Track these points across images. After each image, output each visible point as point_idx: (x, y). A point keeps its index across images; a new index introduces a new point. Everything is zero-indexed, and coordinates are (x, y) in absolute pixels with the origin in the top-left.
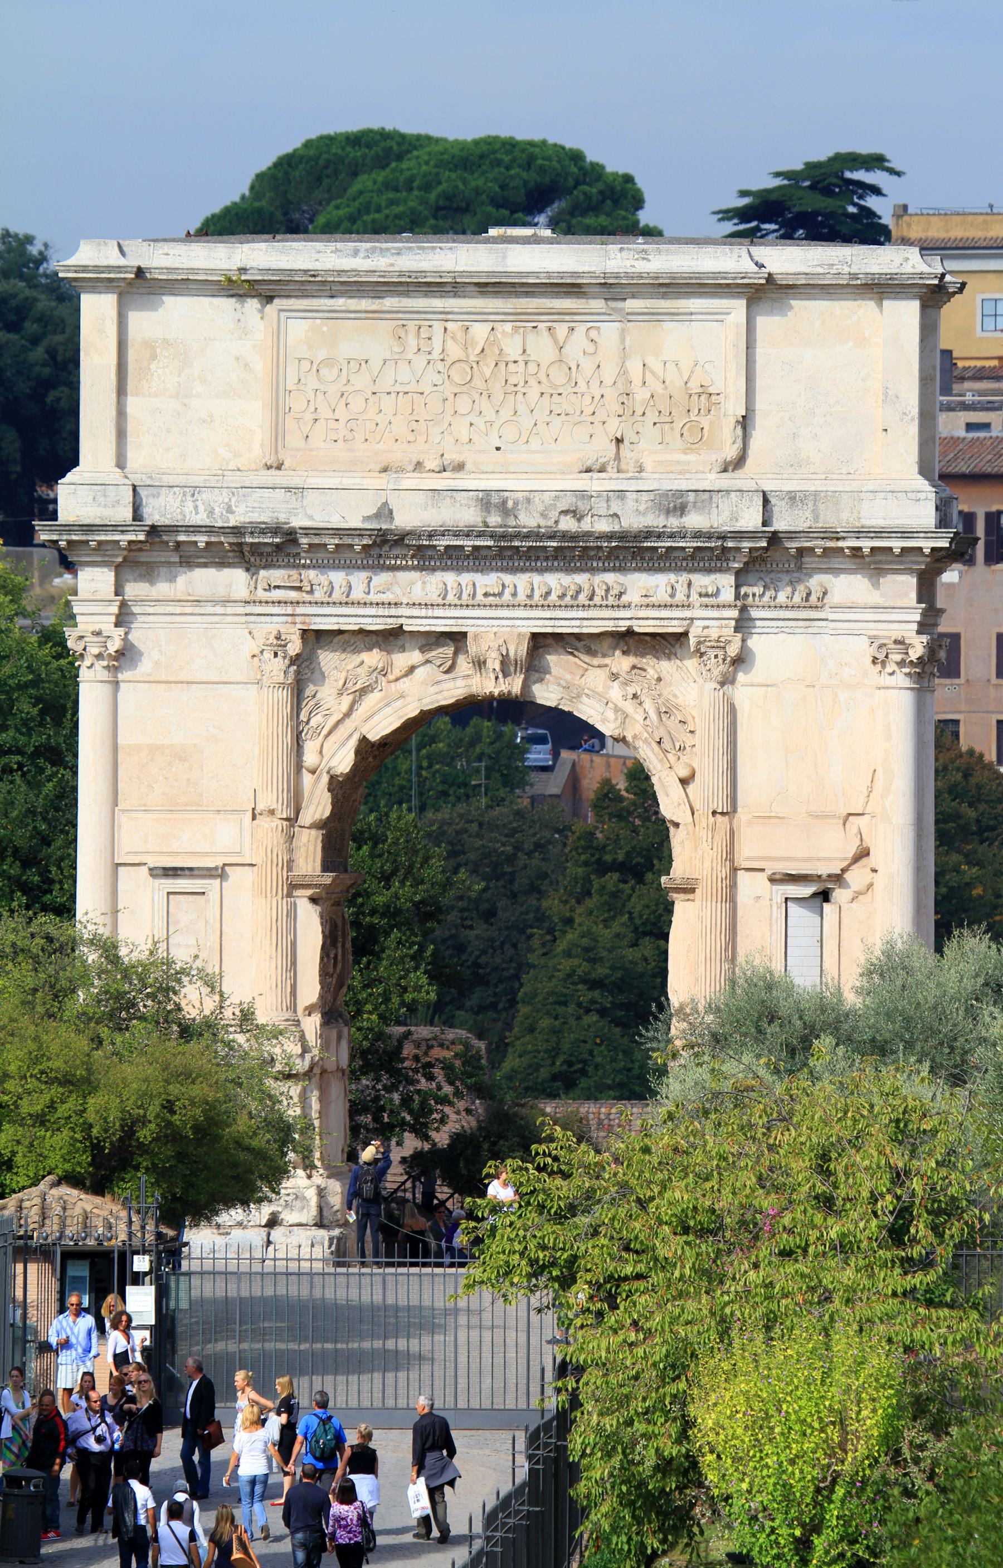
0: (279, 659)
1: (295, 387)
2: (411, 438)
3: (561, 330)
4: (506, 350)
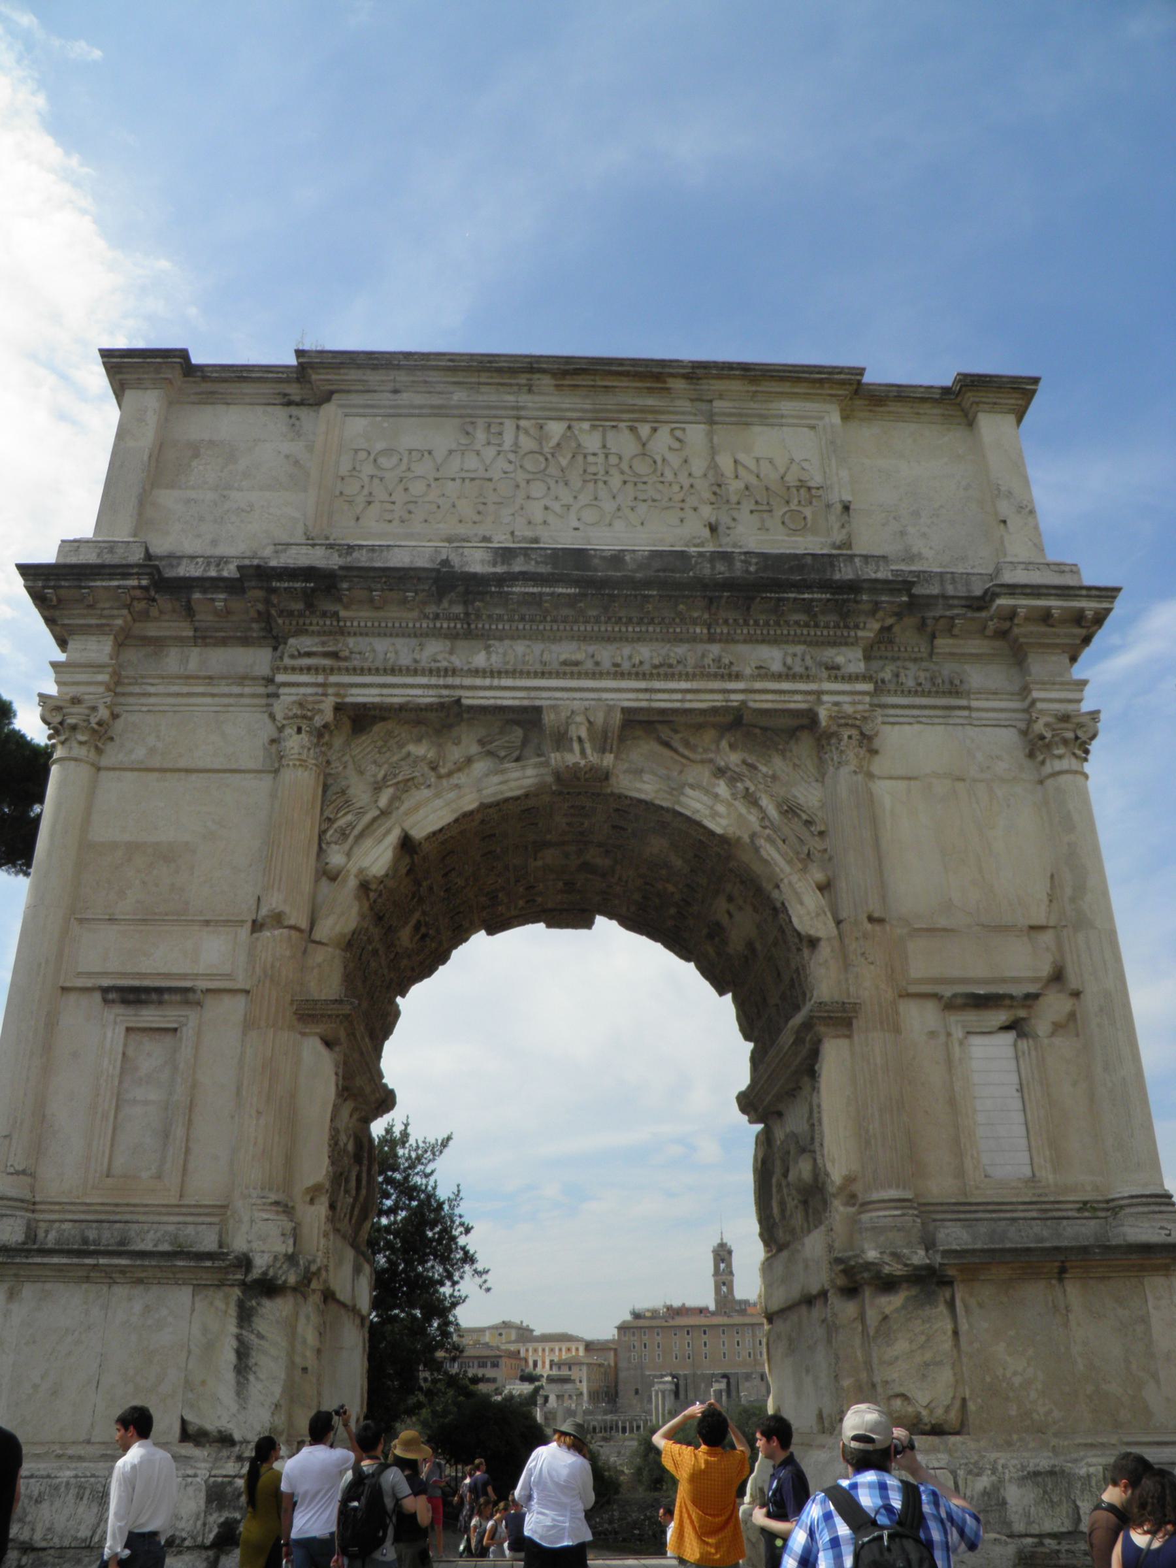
0: (303, 735)
1: (348, 474)
2: (477, 518)
3: (644, 430)
4: (584, 444)
